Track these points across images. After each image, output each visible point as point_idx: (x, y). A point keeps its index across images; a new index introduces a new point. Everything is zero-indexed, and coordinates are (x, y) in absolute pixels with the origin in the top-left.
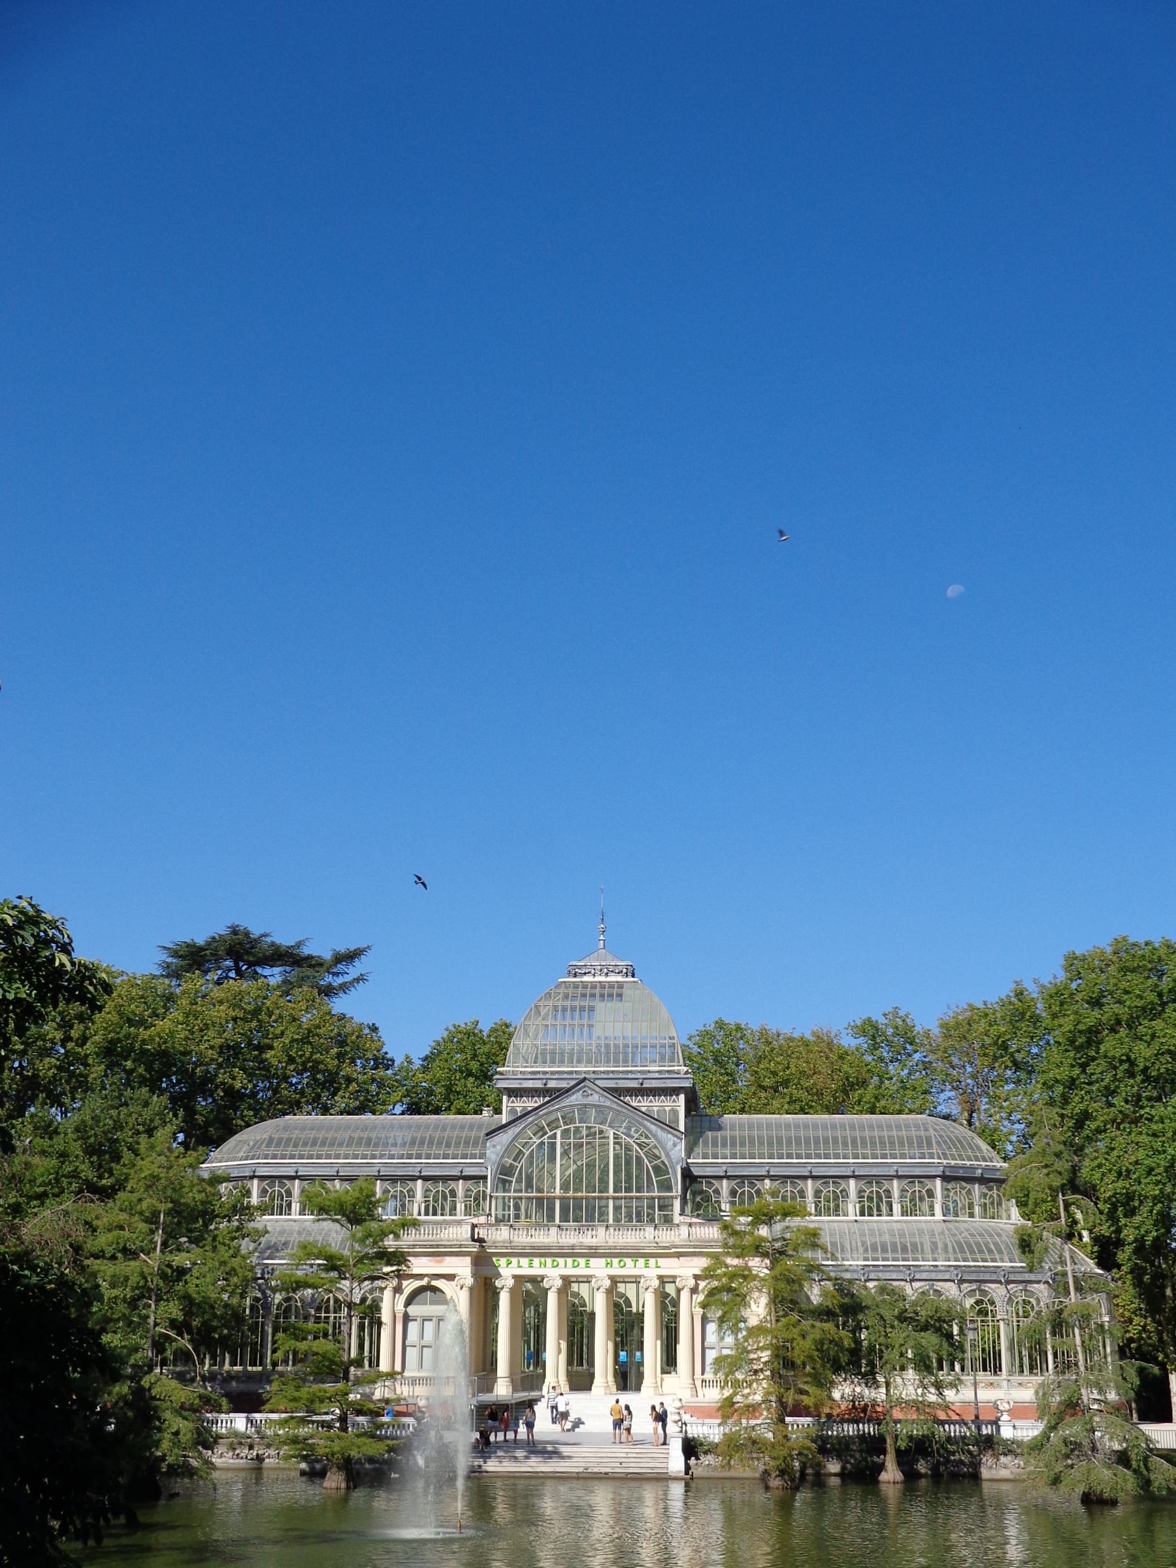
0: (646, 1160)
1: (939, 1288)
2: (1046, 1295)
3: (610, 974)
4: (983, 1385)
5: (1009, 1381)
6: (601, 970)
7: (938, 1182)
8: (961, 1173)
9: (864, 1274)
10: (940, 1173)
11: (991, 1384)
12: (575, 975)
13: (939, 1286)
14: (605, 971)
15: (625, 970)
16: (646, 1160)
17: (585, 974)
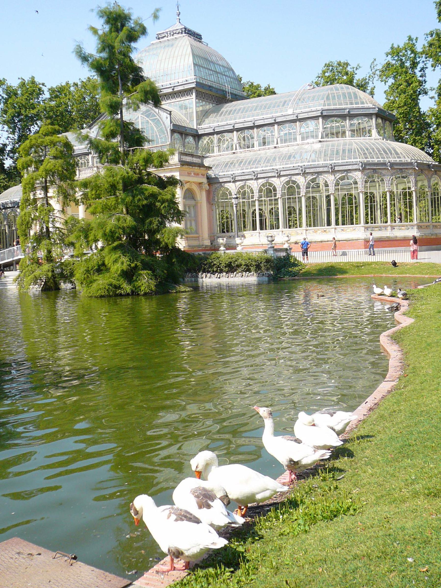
0: (155, 128)
1: (294, 179)
2: (360, 177)
3: (175, 35)
4: (320, 232)
5: (335, 229)
6: (170, 34)
7: (320, 120)
8: (335, 113)
9: (254, 176)
10: (320, 114)
11: (325, 231)
12: (159, 39)
13: (294, 178)
14: (172, 33)
15: (181, 31)
16: (155, 128)
17: (163, 37)
